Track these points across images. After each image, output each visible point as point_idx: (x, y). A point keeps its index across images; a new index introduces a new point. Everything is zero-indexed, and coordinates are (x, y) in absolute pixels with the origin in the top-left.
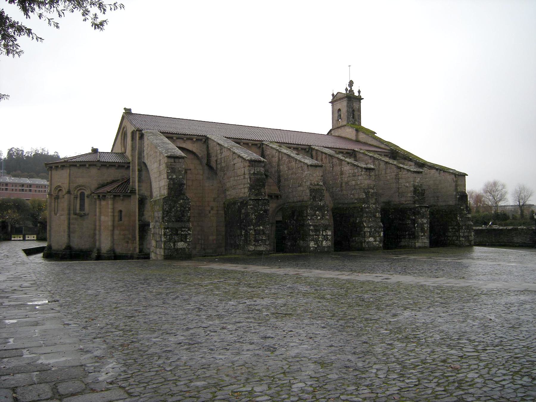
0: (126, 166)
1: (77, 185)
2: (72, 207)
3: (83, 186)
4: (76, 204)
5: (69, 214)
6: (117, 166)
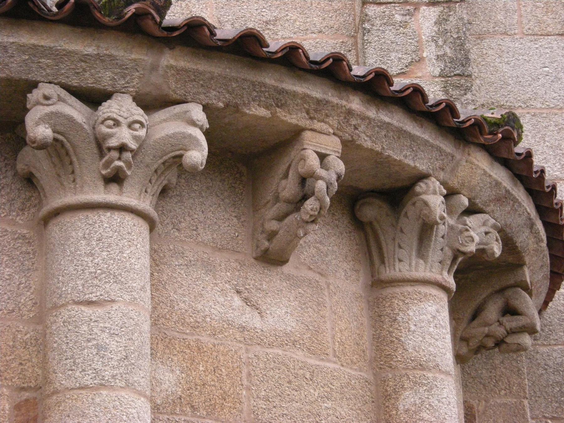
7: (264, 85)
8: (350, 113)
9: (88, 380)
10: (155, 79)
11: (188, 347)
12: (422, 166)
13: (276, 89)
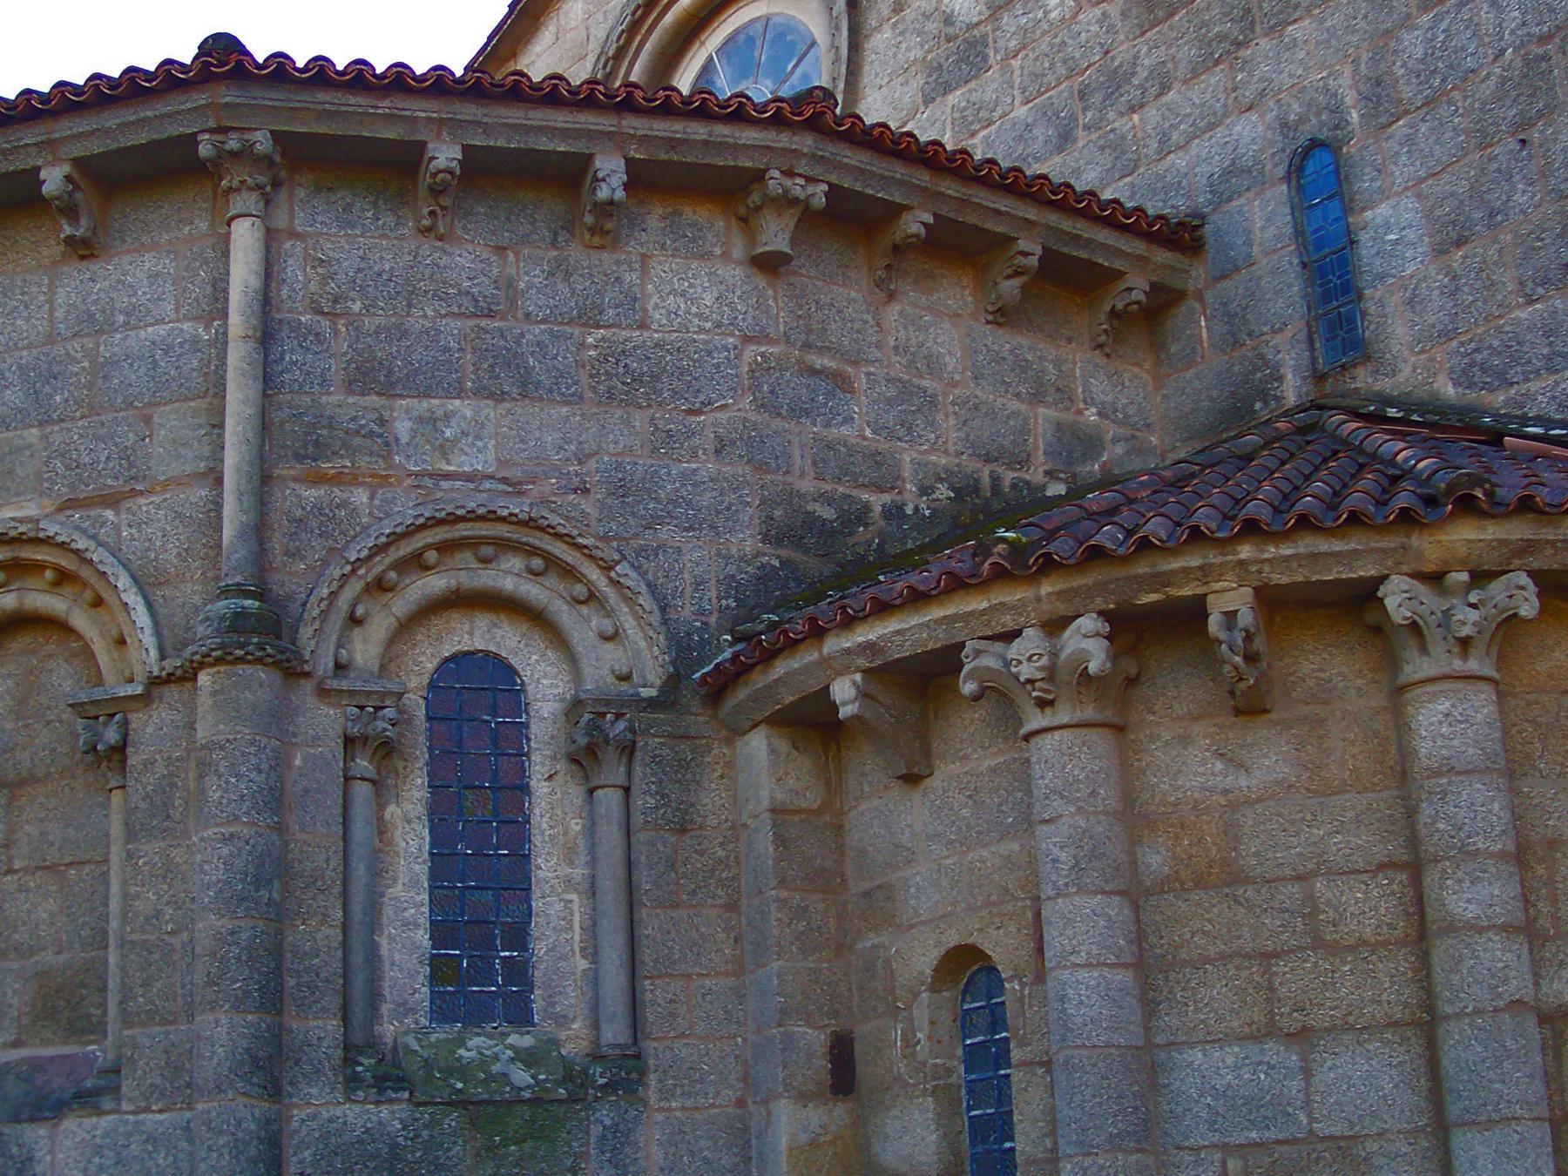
0: (1137, 286)
1: (405, 509)
2: (315, 935)
3: (524, 536)
4: (378, 872)
6: (1031, 248)
7: (1137, 576)
8: (1242, 563)
9: (1051, 893)
10: (1045, 607)
11: (1172, 826)
12: (1368, 570)
13: (1152, 575)
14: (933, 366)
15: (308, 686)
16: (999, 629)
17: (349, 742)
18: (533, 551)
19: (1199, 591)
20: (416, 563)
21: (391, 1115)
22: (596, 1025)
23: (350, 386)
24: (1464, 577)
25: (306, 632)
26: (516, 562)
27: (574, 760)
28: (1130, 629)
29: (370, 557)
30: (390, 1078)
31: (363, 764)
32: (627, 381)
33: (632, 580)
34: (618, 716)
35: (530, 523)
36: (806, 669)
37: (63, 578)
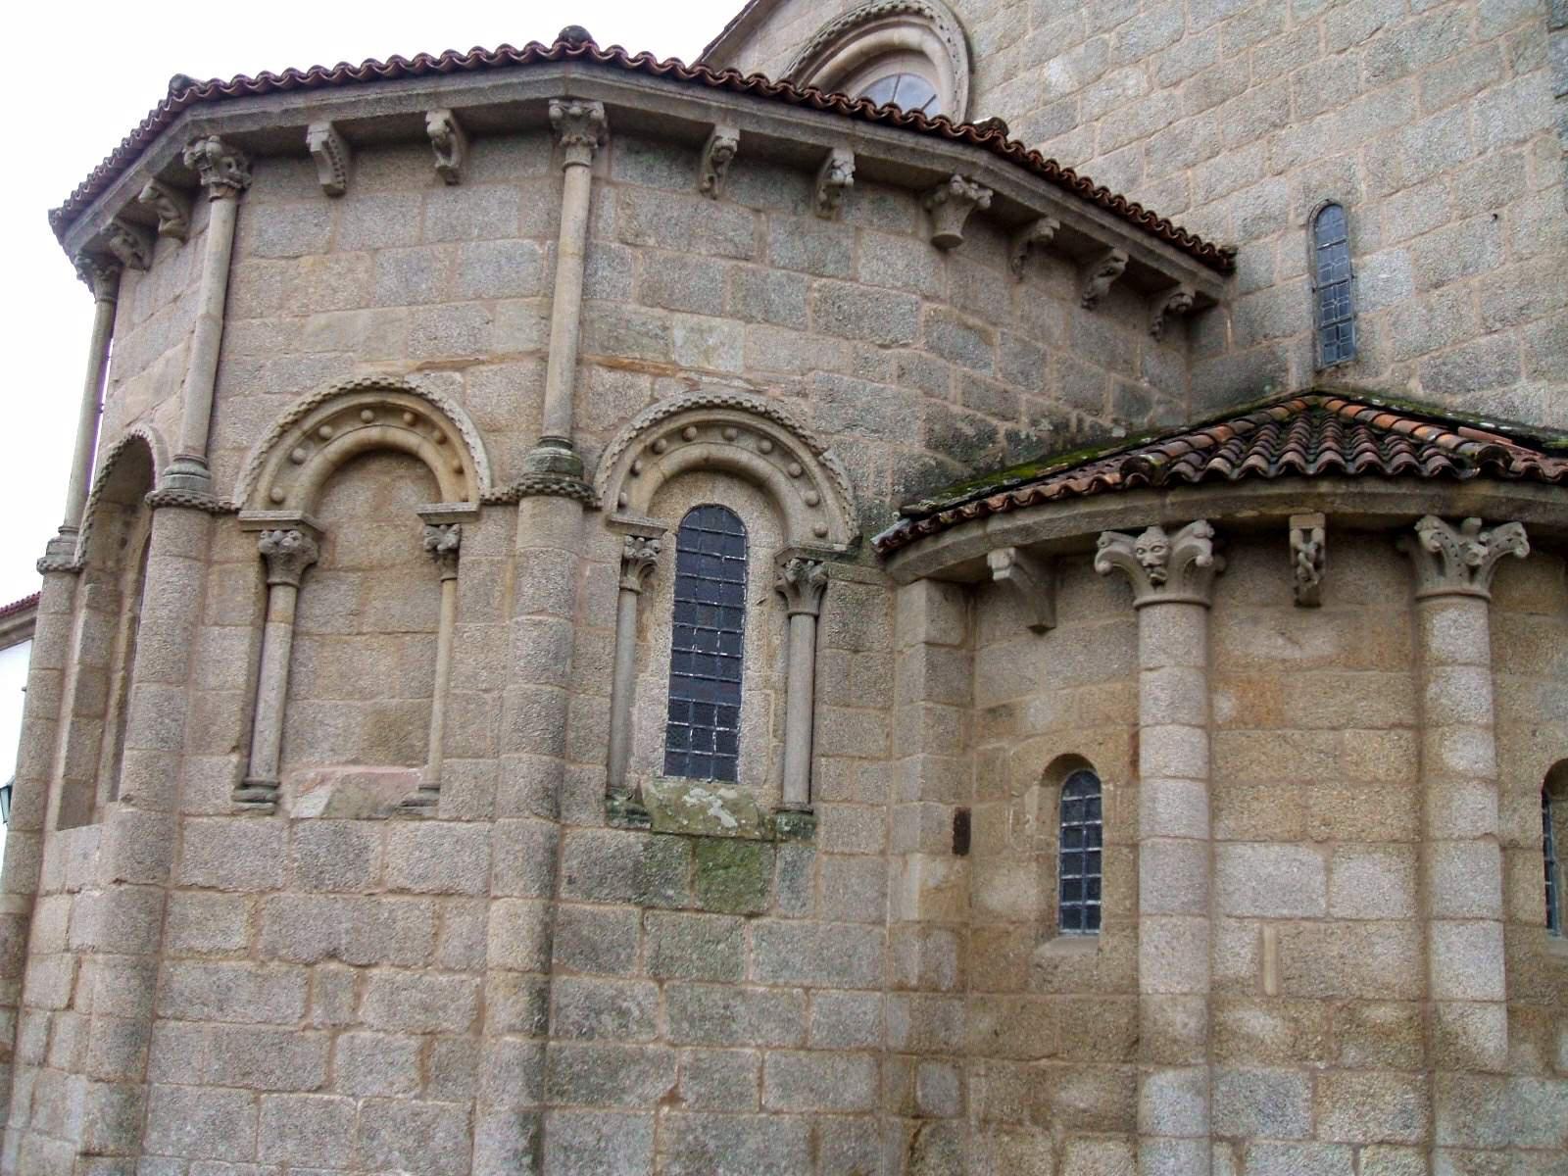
0: (1187, 293)
1: (676, 395)
2: (592, 703)
5: (554, 799)
6: (1121, 255)
8: (1321, 495)
9: (1150, 722)
14: (1046, 335)
15: (600, 518)
16: (1128, 525)
17: (626, 562)
18: (765, 436)
19: (1285, 512)
20: (681, 436)
21: (634, 840)
22: (781, 787)
23: (642, 300)
24: (1478, 522)
25: (600, 477)
26: (750, 443)
27: (780, 593)
28: (1228, 538)
29: (649, 427)
30: (637, 815)
31: (633, 581)
32: (836, 319)
33: (838, 466)
34: (817, 563)
35: (766, 415)
36: (971, 542)
37: (418, 420)
